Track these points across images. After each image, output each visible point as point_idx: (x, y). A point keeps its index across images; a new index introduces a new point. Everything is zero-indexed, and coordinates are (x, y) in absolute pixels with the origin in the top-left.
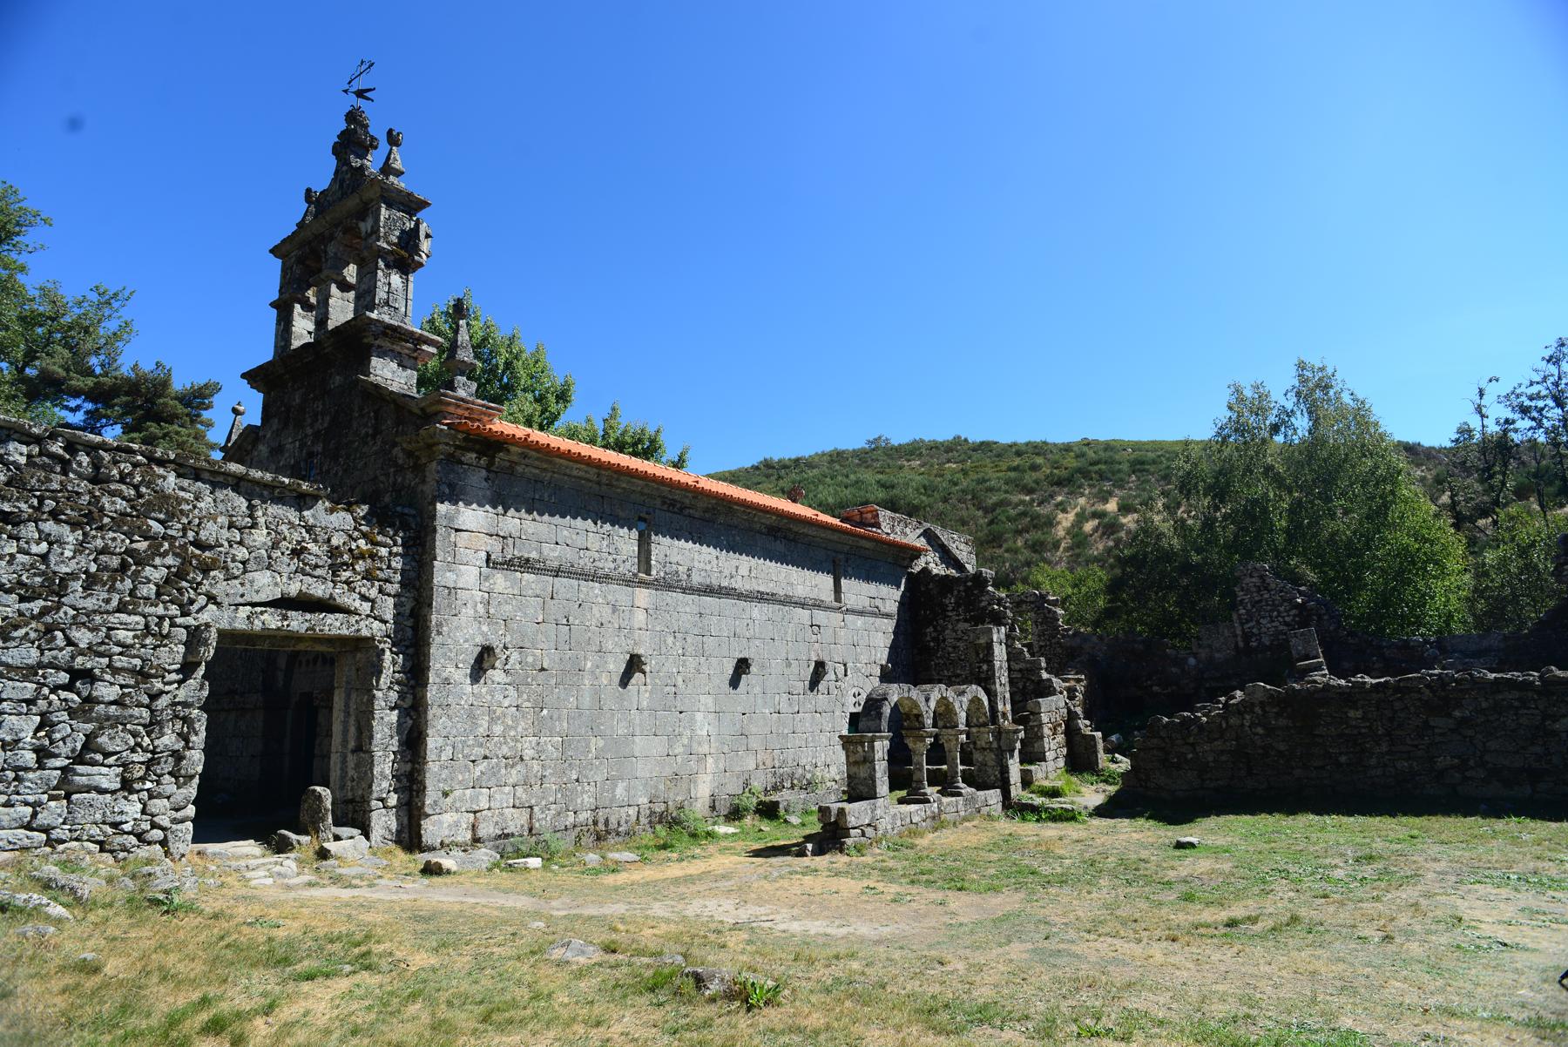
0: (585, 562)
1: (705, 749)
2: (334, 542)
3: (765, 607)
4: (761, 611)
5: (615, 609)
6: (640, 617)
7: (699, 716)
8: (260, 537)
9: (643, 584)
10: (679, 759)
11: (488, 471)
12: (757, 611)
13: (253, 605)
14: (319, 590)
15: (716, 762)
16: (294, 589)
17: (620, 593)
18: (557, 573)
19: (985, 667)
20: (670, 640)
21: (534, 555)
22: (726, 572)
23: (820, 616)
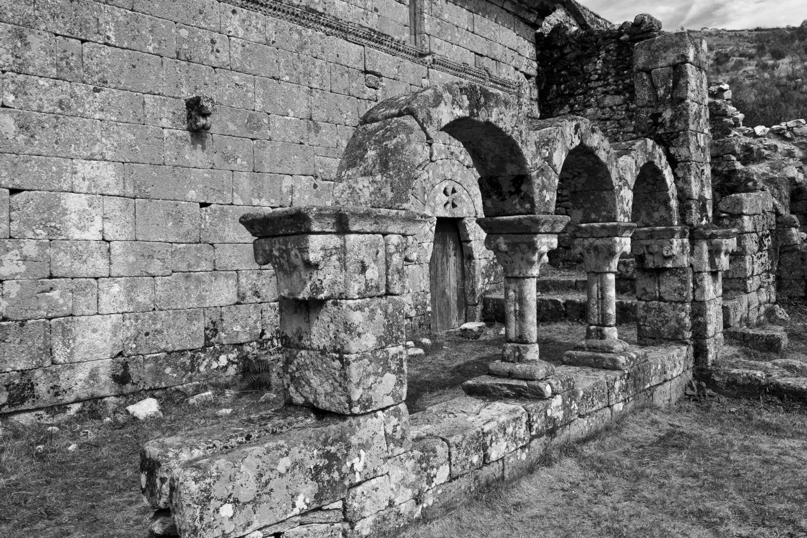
1: (100, 265)
7: (74, 203)
15: (130, 289)
19: (668, 114)
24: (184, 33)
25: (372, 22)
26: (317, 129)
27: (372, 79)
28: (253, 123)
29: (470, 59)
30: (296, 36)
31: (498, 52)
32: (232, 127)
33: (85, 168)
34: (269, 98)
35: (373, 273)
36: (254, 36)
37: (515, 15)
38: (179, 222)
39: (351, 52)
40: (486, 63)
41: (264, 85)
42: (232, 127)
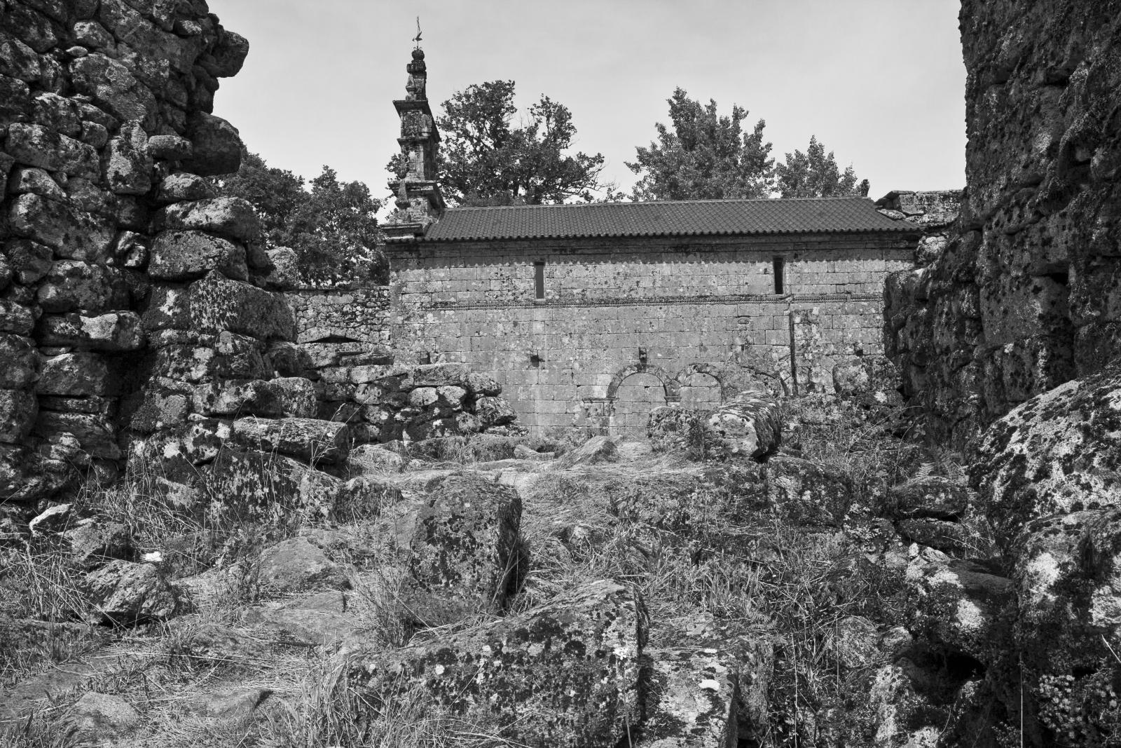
0: (491, 298)
2: (345, 309)
3: (673, 308)
4: (667, 312)
5: (515, 324)
6: (538, 327)
8: (310, 313)
9: (536, 305)
10: (577, 416)
11: (418, 258)
12: (659, 312)
13: (311, 342)
14: (340, 333)
16: (327, 334)
17: (522, 315)
18: (469, 308)
20: (566, 340)
21: (453, 300)
22: (625, 287)
23: (751, 308)
24: (638, 322)
25: (744, 290)
26: (706, 349)
27: (742, 320)
28: (670, 353)
29: (830, 290)
30: (693, 310)
31: (863, 277)
32: (659, 355)
33: (601, 377)
34: (678, 341)
35: (599, 411)
36: (671, 316)
37: (881, 249)
38: (635, 393)
39: (729, 309)
40: (847, 288)
41: (675, 335)
42: (659, 355)
